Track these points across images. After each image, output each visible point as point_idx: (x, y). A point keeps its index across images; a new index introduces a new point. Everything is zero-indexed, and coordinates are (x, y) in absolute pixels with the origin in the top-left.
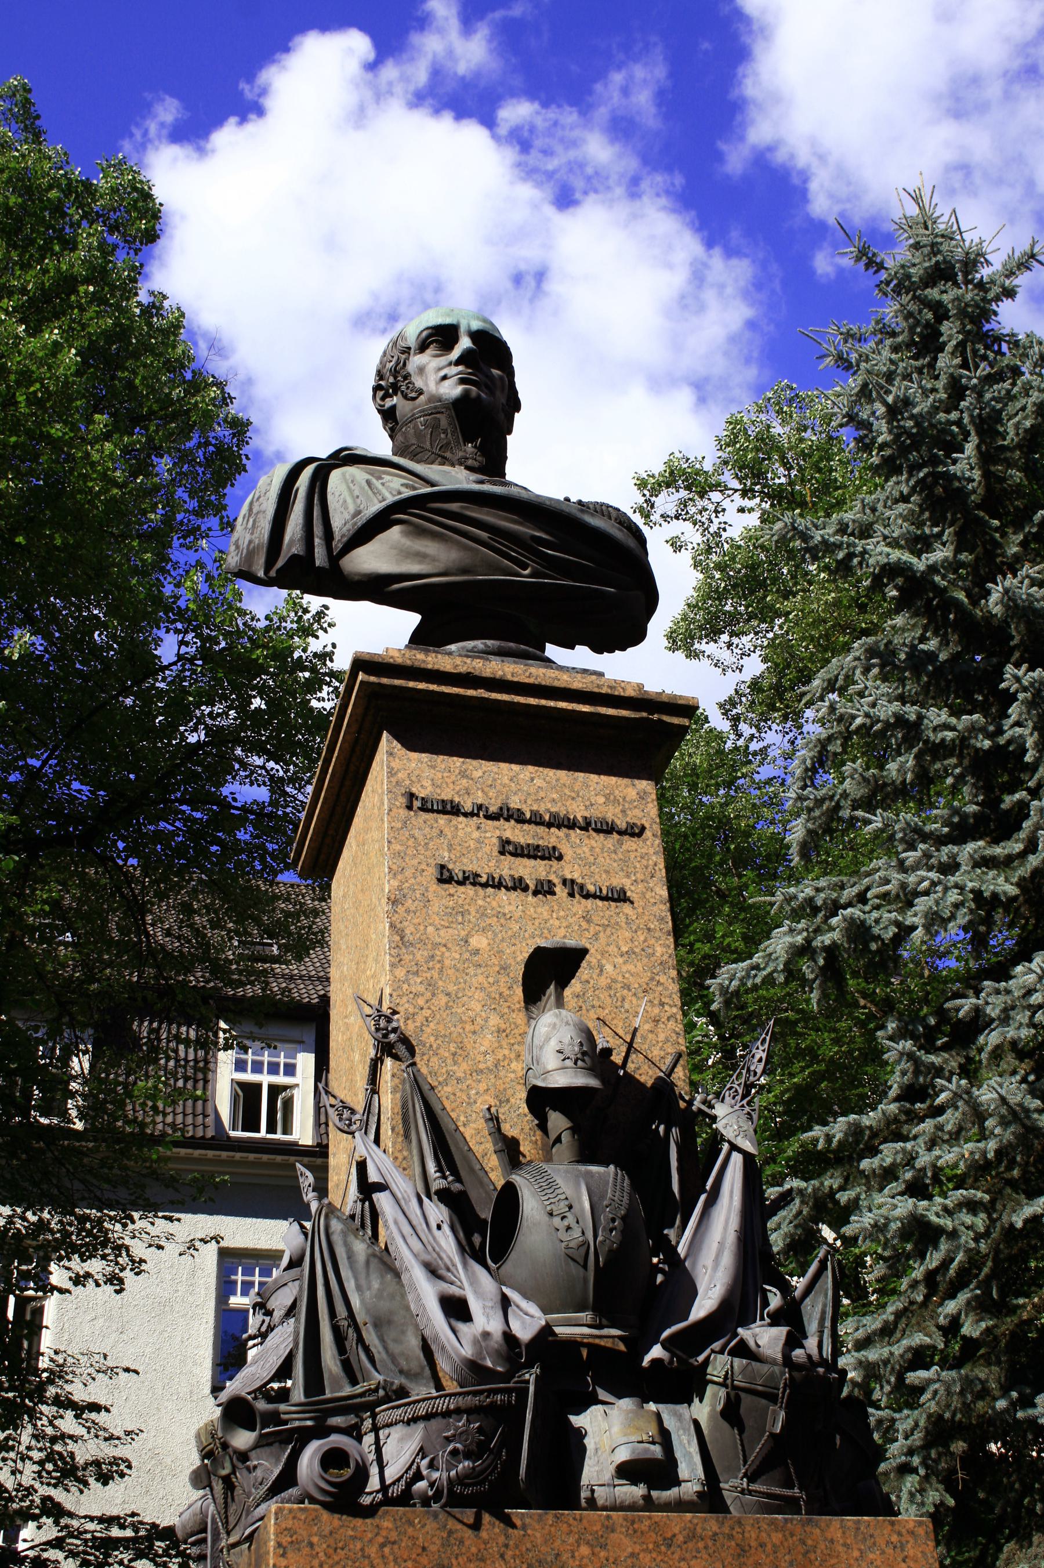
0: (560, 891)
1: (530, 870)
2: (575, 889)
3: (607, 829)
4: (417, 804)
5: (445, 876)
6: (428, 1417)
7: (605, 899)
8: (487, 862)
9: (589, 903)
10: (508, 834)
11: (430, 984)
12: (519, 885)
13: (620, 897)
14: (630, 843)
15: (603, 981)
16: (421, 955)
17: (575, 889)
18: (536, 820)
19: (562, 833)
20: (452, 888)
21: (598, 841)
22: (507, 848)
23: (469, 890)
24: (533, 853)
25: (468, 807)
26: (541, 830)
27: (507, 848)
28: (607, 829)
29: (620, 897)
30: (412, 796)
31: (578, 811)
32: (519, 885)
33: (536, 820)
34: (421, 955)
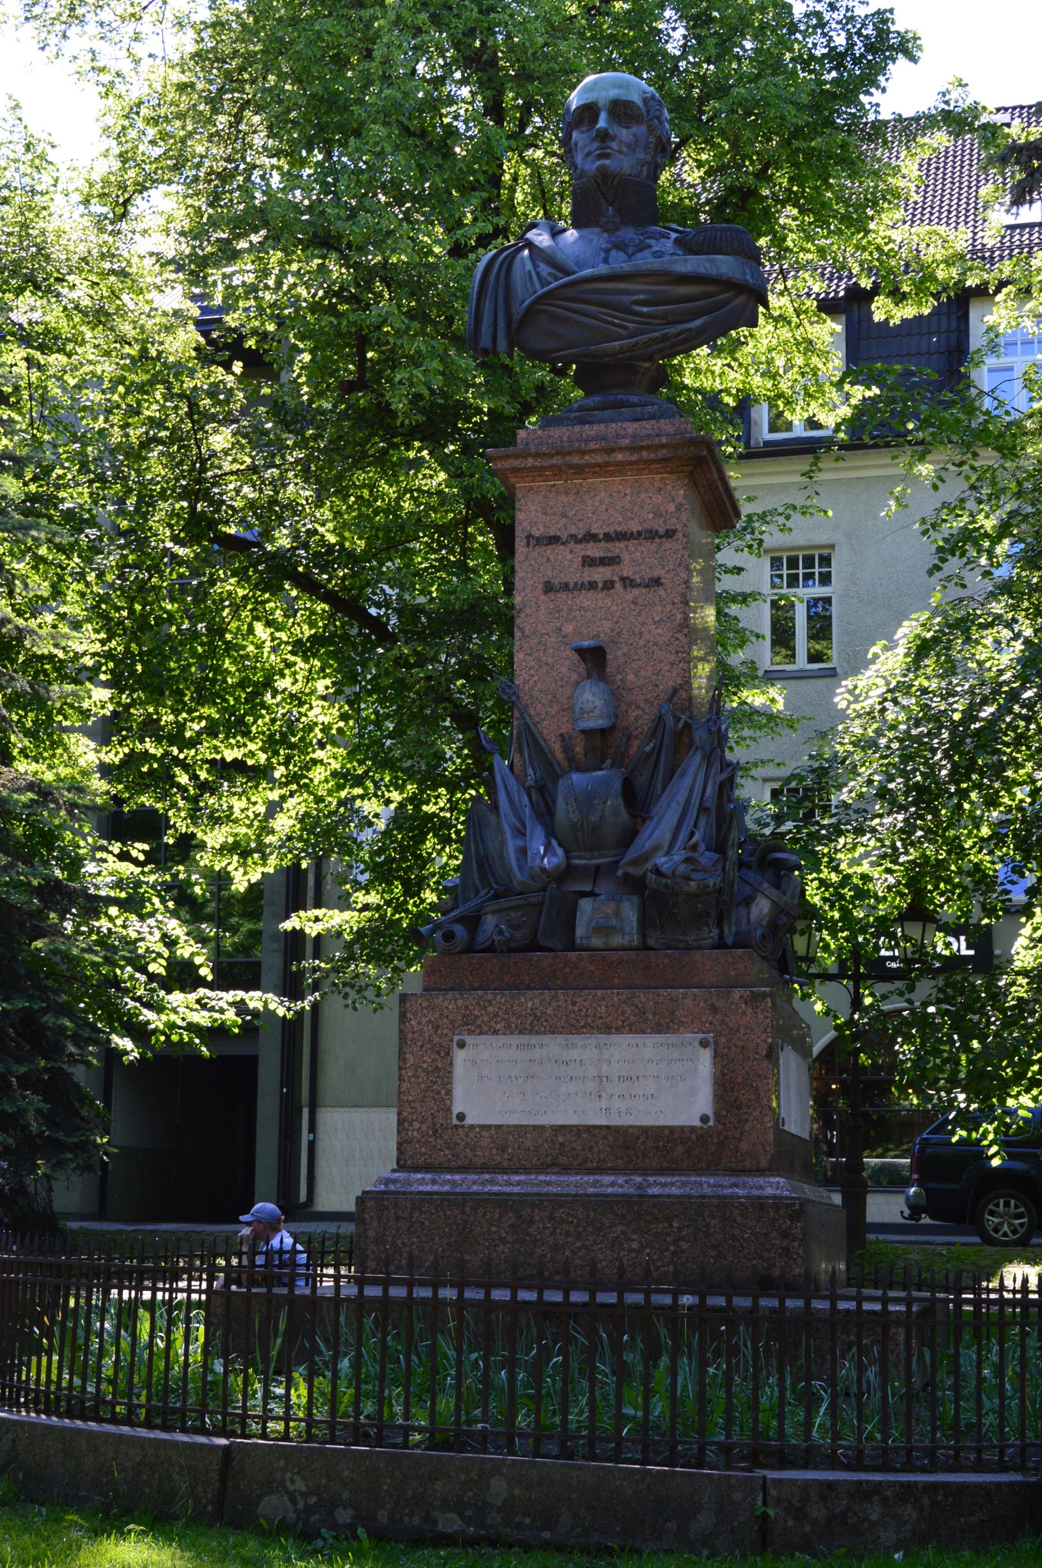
0: (618, 586)
1: (601, 574)
2: (628, 582)
3: (652, 535)
4: (532, 542)
5: (549, 588)
6: (499, 911)
7: (647, 586)
8: (574, 574)
9: (636, 591)
10: (589, 553)
11: (538, 660)
12: (592, 586)
13: (657, 582)
14: (667, 544)
15: (642, 643)
16: (533, 642)
17: (628, 582)
18: (608, 538)
19: (622, 545)
20: (552, 595)
21: (648, 547)
22: (589, 562)
23: (564, 596)
24: (604, 561)
25: (564, 538)
26: (610, 545)
27: (589, 562)
28: (652, 535)
29: (657, 582)
30: (529, 537)
31: (635, 527)
32: (592, 586)
33: (608, 538)
34: (533, 642)
